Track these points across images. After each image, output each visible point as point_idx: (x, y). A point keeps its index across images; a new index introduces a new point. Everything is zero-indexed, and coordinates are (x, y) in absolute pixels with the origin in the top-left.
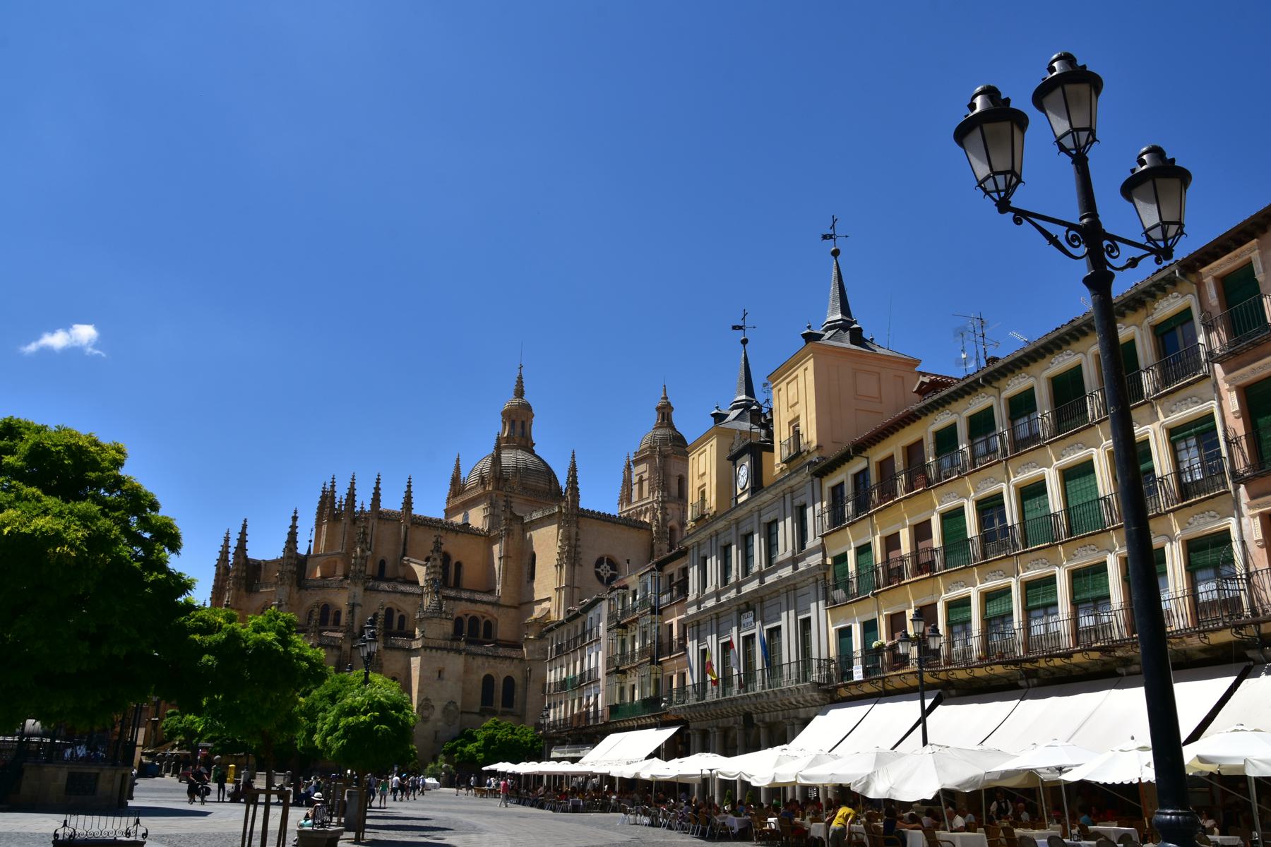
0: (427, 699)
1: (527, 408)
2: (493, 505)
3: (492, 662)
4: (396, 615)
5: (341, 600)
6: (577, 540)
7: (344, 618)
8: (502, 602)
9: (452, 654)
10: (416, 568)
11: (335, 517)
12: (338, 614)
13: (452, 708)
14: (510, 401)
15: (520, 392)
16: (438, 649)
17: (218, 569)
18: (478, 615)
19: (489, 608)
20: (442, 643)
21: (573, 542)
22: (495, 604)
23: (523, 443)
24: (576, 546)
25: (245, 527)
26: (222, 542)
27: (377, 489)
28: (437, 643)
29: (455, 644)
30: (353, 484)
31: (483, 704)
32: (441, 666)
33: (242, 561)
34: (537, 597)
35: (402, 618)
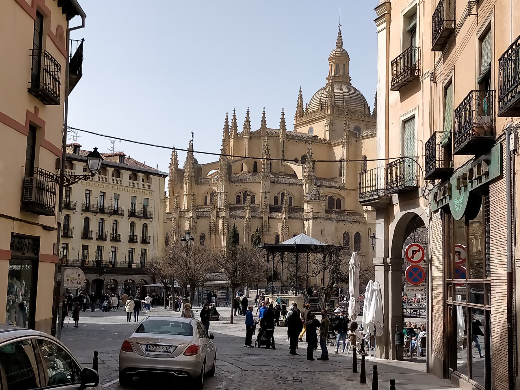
3: (348, 224)
9: (328, 221)
11: (238, 136)
27: (264, 117)
30: (248, 114)
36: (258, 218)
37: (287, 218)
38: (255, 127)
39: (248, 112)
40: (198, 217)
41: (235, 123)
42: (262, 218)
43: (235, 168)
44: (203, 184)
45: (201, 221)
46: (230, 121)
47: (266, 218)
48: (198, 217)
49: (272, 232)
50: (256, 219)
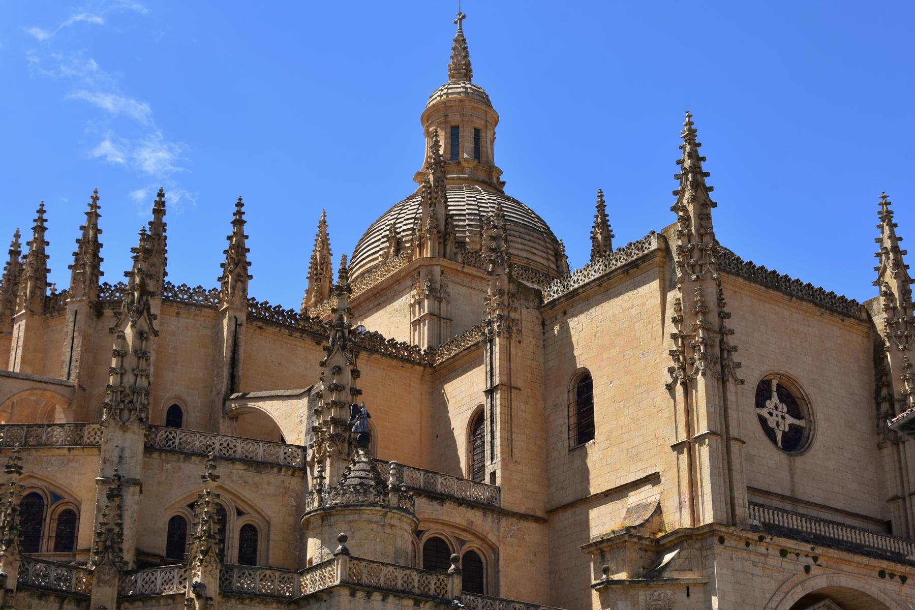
1: (484, 99)
2: (436, 293)
4: (235, 525)
5: (80, 480)
8: (506, 501)
10: (275, 409)
12: (70, 519)
14: (442, 89)
18: (446, 534)
19: (475, 517)
20: (399, 577)
21: (714, 319)
22: (489, 507)
23: (482, 175)
28: (385, 575)
29: (433, 581)
30: (93, 216)
34: (597, 486)
35: (249, 534)
39: (94, 206)
41: (40, 256)
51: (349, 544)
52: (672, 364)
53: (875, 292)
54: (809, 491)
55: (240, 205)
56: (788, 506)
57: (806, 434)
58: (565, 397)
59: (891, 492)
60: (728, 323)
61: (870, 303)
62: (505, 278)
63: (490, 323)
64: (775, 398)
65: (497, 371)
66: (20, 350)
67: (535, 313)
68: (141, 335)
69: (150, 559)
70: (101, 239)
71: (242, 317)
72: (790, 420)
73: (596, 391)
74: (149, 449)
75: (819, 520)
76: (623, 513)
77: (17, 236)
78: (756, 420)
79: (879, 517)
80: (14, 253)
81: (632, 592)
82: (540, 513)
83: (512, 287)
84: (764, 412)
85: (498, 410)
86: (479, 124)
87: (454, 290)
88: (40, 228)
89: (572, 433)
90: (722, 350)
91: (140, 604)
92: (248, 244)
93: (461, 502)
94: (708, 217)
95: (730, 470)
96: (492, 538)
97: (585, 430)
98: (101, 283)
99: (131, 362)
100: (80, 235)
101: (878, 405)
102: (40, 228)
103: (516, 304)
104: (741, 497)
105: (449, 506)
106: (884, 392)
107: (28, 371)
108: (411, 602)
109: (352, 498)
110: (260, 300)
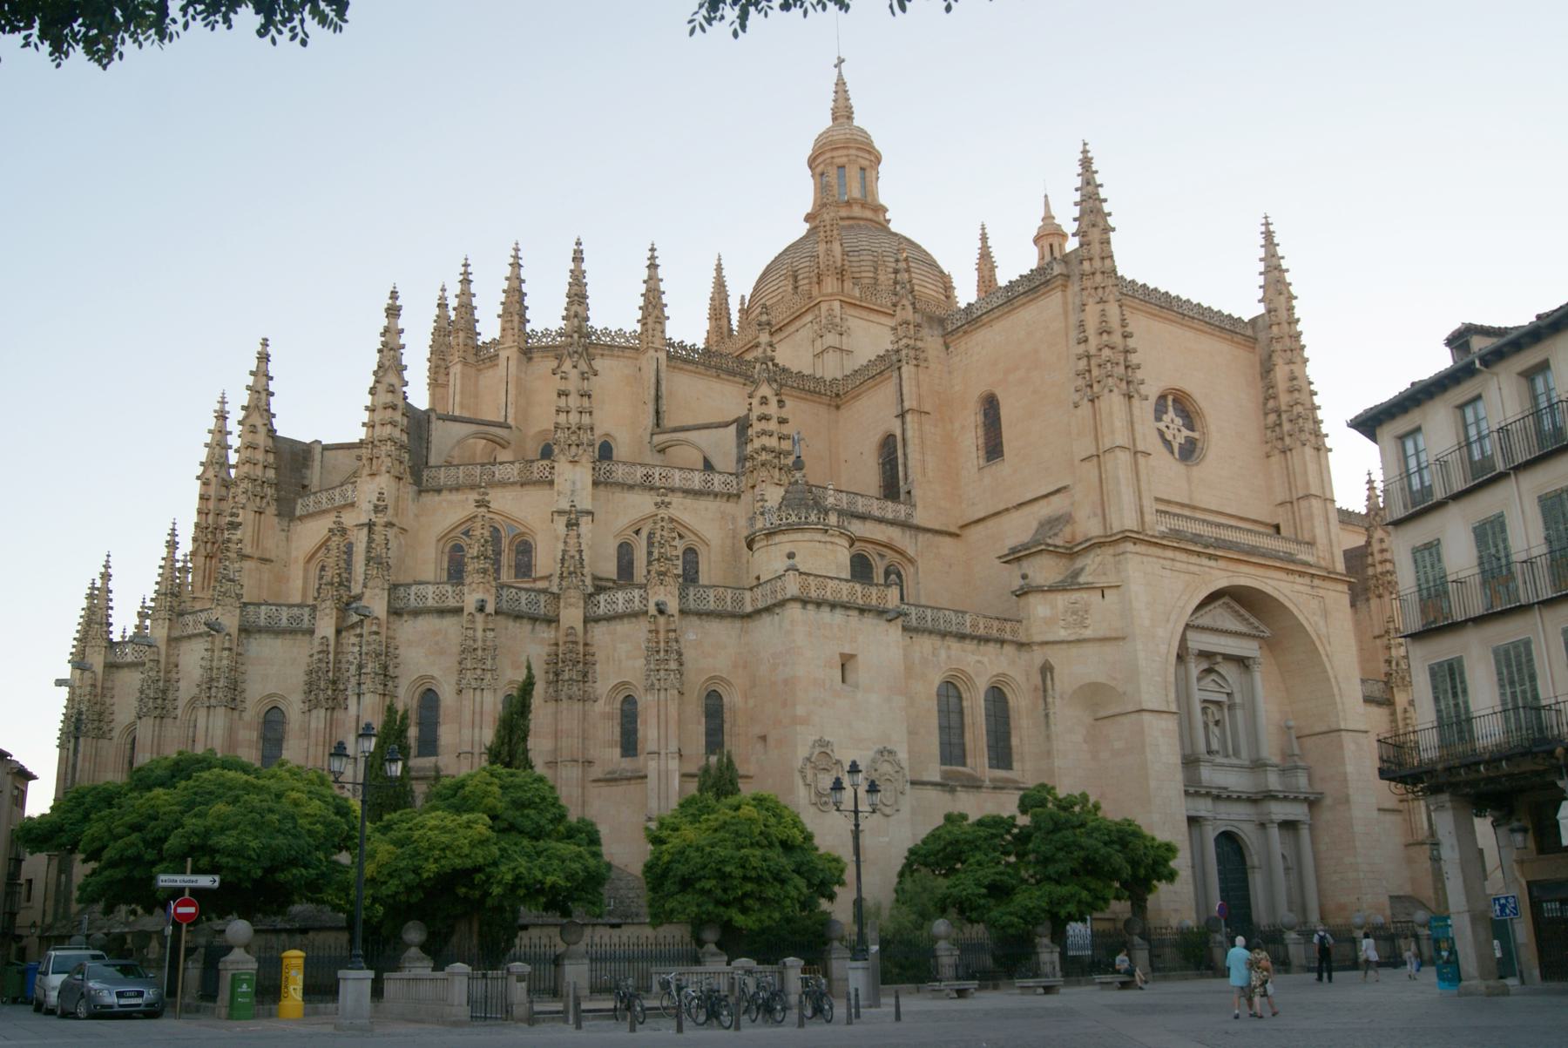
0: (822, 743)
3: (955, 645)
6: (1126, 336)
7: (545, 560)
9: (869, 621)
11: (482, 356)
12: (525, 549)
13: (886, 768)
15: (842, 111)
16: (833, 606)
17: (206, 484)
21: (1117, 339)
24: (1127, 352)
25: (264, 358)
26: (212, 423)
31: (943, 762)
32: (847, 650)
33: (261, 439)
36: (534, 619)
37: (673, 606)
38: (546, 314)
39: (516, 257)
40: (246, 630)
41: (467, 307)
42: (552, 621)
43: (443, 437)
44: (311, 515)
45: (265, 649)
46: (453, 302)
47: (571, 615)
48: (246, 630)
49: (605, 680)
50: (526, 626)
51: (798, 561)
52: (1080, 382)
53: (1260, 309)
54: (1205, 499)
55: (653, 250)
56: (1187, 512)
57: (1199, 445)
58: (973, 418)
59: (1281, 495)
60: (1131, 343)
61: (1254, 321)
62: (910, 308)
63: (898, 351)
64: (1171, 413)
65: (906, 397)
66: (458, 398)
67: (941, 340)
68: (583, 377)
69: (603, 583)
70: (525, 288)
71: (662, 356)
72: (1185, 432)
73: (1004, 412)
74: (595, 484)
75: (1218, 525)
76: (1035, 525)
77: (443, 290)
78: (1156, 433)
79: (1268, 521)
80: (442, 306)
81: (1051, 596)
82: (953, 529)
83: (918, 318)
84: (1162, 425)
85: (909, 434)
86: (865, 163)
87: (853, 323)
88: (466, 281)
89: (982, 453)
90: (1127, 367)
91: (604, 623)
92: (663, 286)
93: (881, 520)
94: (1108, 242)
95: (1138, 480)
96: (911, 552)
97: (993, 449)
98: (528, 329)
99: (573, 401)
100: (505, 285)
101: (1266, 414)
102: (466, 281)
103: (925, 332)
104: (1150, 506)
105: (869, 525)
106: (1271, 404)
107: (466, 414)
108: (855, 613)
109: (794, 519)
110: (676, 339)
